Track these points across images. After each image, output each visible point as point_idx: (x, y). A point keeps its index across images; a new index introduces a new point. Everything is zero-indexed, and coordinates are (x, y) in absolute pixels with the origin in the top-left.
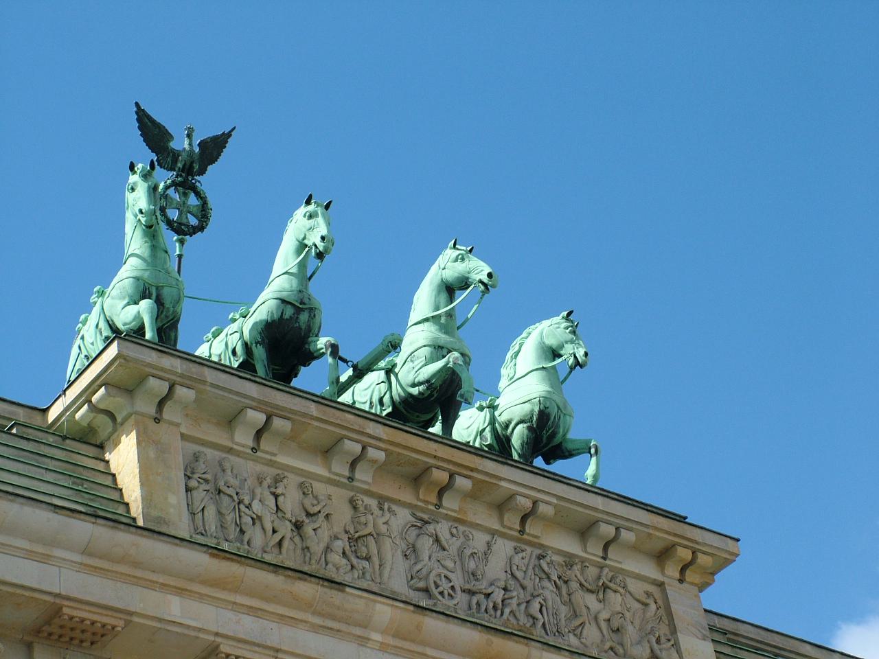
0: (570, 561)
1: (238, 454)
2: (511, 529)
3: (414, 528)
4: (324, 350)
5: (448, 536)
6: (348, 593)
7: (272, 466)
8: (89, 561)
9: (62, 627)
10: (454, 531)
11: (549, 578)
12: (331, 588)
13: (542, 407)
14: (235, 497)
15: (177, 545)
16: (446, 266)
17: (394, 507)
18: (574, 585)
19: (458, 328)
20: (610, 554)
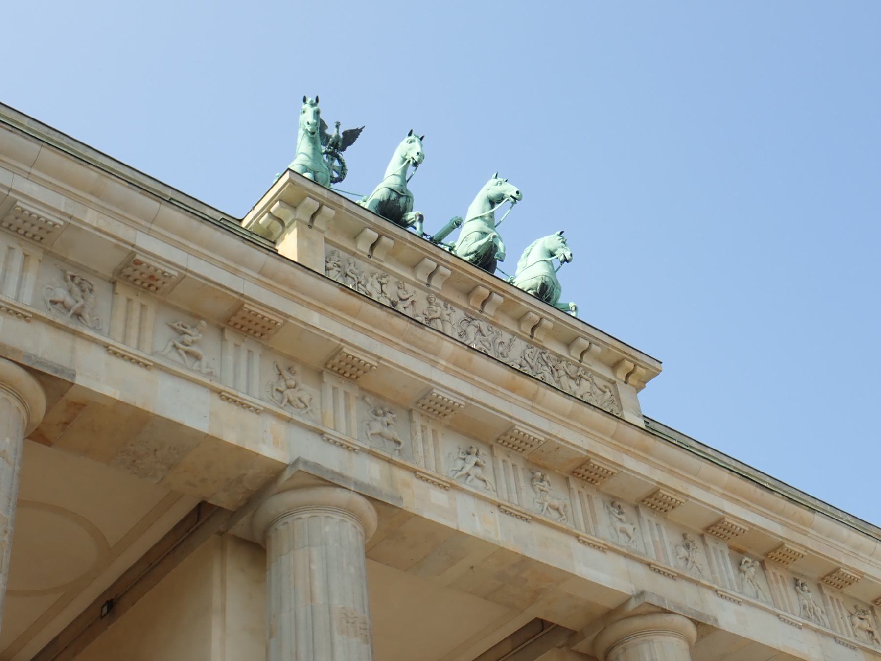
0: (560, 358)
1: (359, 257)
2: (525, 333)
3: (465, 321)
4: (414, 219)
5: (487, 330)
6: (427, 331)
7: (380, 269)
8: (264, 279)
9: (243, 318)
10: (491, 329)
11: (547, 365)
12: (416, 326)
13: (543, 281)
14: (356, 278)
15: (319, 278)
16: (491, 188)
17: (454, 308)
18: (562, 372)
19: (496, 226)
20: (584, 359)
